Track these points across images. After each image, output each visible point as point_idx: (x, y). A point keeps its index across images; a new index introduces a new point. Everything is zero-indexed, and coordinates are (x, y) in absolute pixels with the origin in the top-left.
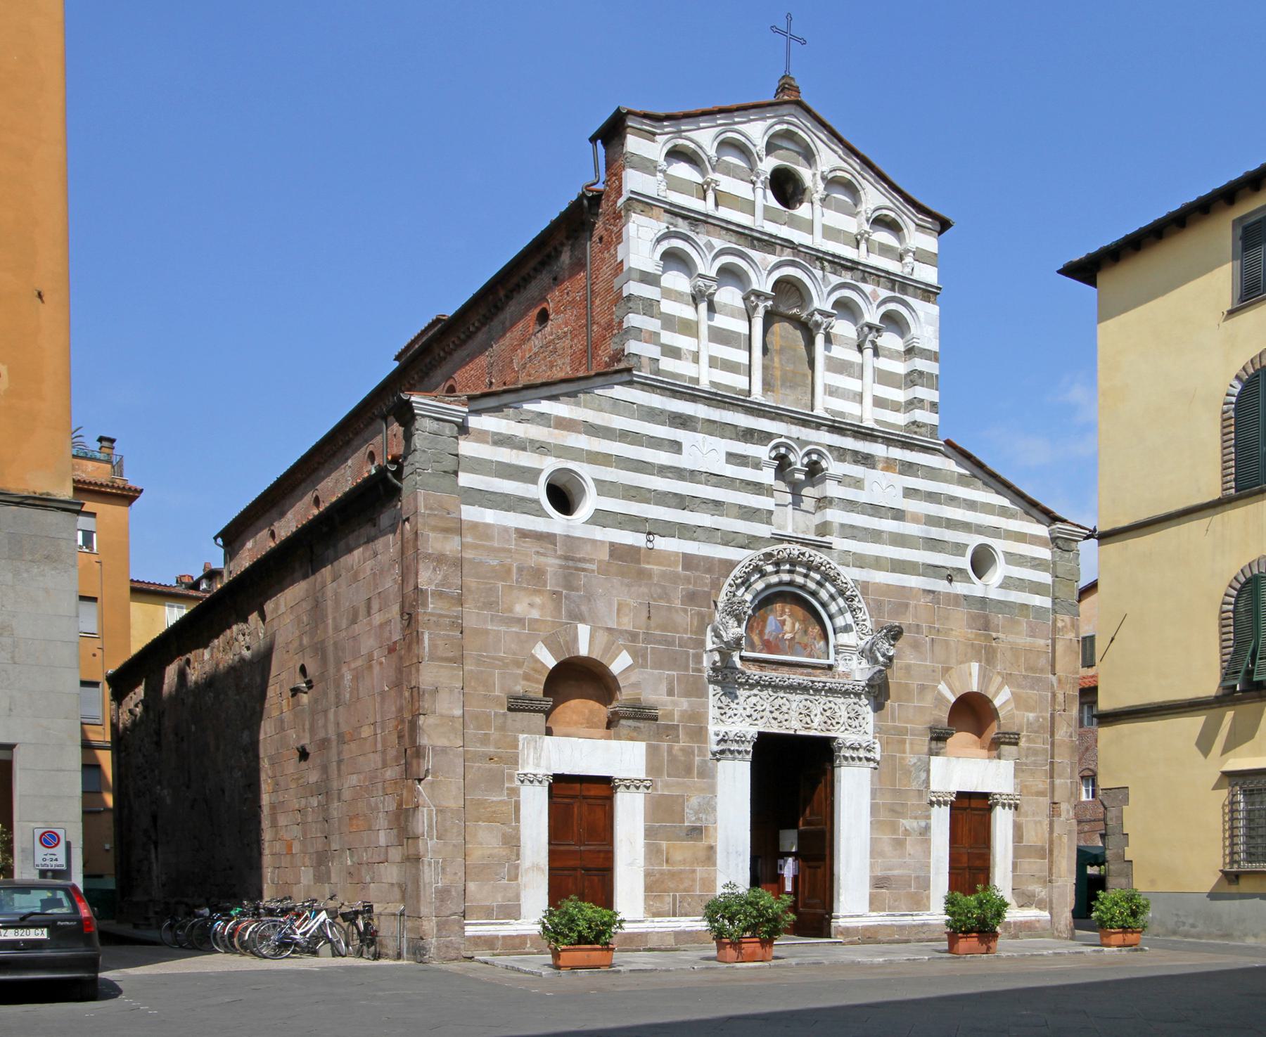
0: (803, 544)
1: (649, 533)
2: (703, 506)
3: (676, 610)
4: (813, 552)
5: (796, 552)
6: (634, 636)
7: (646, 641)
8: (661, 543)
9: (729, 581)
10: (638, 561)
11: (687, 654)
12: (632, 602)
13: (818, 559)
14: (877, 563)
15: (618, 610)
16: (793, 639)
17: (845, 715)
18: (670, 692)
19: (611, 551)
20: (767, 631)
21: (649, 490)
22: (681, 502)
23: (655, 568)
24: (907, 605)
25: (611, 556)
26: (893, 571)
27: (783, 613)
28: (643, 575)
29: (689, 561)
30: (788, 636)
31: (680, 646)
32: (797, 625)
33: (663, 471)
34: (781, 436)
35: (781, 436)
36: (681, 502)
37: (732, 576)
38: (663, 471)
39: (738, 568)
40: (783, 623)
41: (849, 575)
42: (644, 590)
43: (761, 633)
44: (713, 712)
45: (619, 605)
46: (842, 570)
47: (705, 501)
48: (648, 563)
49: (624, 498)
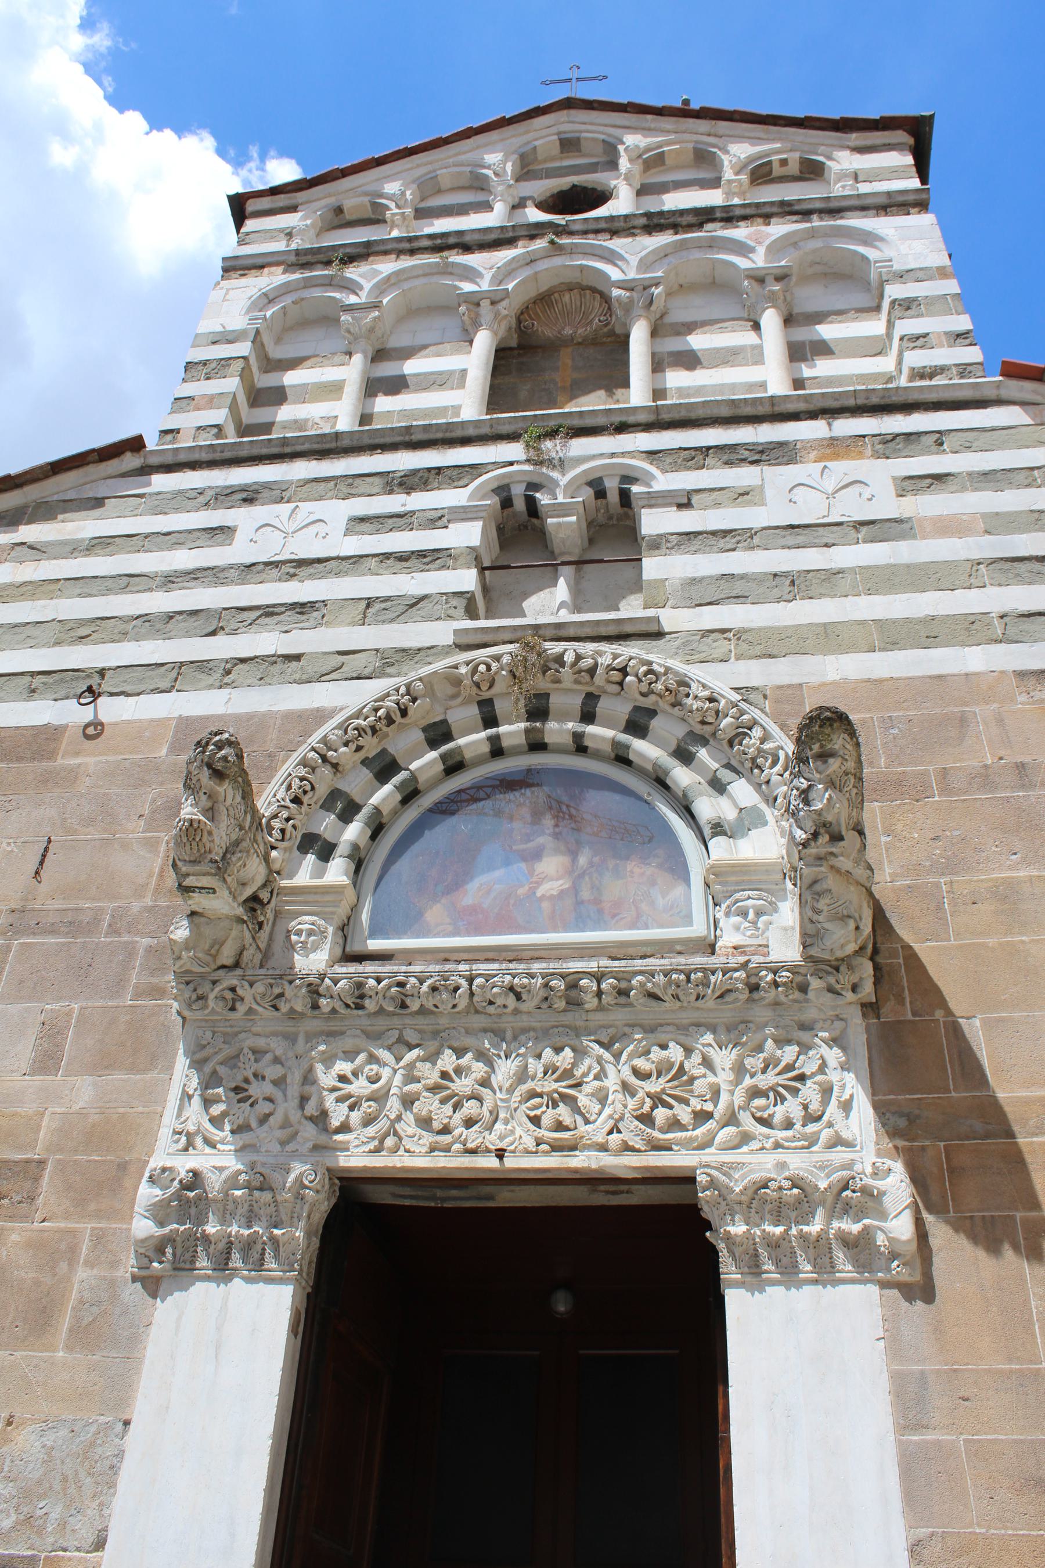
3: (125, 846)
4: (588, 648)
8: (112, 710)
10: (51, 756)
11: (130, 951)
13: (605, 660)
14: (829, 638)
17: (724, 1078)
18: (46, 1062)
24: (963, 721)
31: (113, 930)
33: (170, 580)
34: (511, 464)
35: (511, 464)
38: (170, 580)
41: (718, 678)
46: (695, 672)
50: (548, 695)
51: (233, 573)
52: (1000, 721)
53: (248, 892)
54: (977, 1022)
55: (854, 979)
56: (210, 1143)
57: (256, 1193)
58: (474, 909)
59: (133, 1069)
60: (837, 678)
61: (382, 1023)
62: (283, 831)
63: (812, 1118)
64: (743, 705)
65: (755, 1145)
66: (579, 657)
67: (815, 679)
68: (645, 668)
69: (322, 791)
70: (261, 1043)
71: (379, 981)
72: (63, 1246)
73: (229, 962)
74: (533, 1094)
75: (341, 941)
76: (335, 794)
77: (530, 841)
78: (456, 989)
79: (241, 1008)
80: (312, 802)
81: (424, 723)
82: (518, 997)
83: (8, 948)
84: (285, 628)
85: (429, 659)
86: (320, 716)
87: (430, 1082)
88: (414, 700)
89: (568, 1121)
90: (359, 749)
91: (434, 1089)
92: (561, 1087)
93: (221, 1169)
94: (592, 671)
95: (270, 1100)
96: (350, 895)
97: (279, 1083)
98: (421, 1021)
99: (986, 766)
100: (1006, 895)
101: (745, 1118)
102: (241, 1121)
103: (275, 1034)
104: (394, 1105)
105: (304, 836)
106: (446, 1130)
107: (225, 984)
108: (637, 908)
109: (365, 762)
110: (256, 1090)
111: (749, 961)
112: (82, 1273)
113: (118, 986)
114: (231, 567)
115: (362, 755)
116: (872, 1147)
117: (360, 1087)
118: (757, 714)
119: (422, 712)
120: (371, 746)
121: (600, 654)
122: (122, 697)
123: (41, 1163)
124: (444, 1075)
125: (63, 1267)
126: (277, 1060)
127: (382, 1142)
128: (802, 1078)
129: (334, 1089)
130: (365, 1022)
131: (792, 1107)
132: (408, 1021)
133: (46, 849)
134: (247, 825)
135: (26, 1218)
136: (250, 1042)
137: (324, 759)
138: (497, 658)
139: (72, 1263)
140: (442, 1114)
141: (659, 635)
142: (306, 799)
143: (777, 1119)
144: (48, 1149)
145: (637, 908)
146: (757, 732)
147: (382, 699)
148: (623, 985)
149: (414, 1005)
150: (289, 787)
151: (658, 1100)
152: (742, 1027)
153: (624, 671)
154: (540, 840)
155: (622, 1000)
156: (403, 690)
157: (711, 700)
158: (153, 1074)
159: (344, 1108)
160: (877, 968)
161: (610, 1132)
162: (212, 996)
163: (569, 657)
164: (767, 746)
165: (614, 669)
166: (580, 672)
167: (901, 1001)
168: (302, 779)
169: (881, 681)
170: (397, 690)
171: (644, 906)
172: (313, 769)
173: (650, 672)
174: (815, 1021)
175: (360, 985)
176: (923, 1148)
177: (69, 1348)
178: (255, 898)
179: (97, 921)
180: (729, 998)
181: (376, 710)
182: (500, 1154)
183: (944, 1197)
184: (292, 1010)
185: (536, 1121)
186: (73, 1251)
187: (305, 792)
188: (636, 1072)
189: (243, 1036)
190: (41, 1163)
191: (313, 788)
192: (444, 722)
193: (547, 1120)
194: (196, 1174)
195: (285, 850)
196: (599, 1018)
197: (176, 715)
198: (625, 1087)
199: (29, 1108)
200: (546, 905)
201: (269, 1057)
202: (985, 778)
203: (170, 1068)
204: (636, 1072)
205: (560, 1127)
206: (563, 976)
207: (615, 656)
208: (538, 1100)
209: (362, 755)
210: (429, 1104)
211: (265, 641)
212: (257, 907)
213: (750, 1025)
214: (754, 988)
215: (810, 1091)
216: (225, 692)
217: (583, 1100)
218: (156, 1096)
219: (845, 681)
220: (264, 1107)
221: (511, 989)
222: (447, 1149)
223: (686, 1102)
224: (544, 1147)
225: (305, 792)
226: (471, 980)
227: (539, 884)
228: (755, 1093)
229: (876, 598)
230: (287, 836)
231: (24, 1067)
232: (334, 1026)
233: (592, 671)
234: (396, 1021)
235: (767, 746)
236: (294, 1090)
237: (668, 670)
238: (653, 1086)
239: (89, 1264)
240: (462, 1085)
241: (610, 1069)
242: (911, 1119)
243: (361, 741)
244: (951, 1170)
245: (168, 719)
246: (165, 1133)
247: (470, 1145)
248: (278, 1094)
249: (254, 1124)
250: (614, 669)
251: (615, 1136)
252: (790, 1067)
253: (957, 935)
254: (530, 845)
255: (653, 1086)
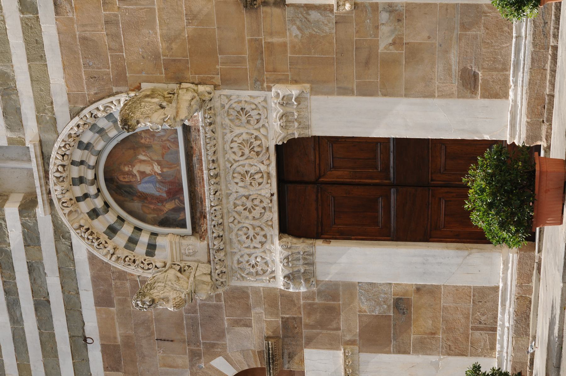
0: (47, 177)
1: (85, 339)
2: (39, 281)
5: (58, 188)
6: (195, 356)
7: (197, 343)
9: (112, 263)
10: (116, 347)
12: (160, 355)
15: (170, 367)
16: (159, 163)
19: (113, 370)
20: (157, 194)
21: (41, 334)
22: (42, 305)
23: (119, 333)
24: (84, 39)
25: (118, 370)
26: (42, 57)
27: (130, 173)
28: (128, 343)
29: (103, 300)
30: (157, 169)
31: (195, 312)
32: (141, 157)
36: (42, 305)
37: (106, 260)
39: (95, 253)
40: (143, 173)
42: (144, 342)
43: (160, 200)
44: (261, 284)
45: (165, 366)
47: (33, 281)
48: (115, 338)
49: (57, 357)
50: (72, 178)
51: (12, 297)
52: (83, 26)
53: (179, 274)
54: (219, 56)
55: (206, 94)
56: (273, 272)
57: (290, 260)
58: (168, 192)
59: (248, 297)
60: (63, 81)
61: (226, 228)
62: (148, 264)
63: (257, 108)
64: (82, 115)
65: (267, 125)
66: (58, 171)
67: (65, 89)
68: (63, 149)
69: (127, 252)
70: (235, 262)
71: (213, 232)
72: (309, 307)
73: (209, 277)
74: (251, 184)
75: (189, 237)
76: (126, 247)
77: (136, 175)
78: (215, 210)
79: (224, 270)
80: (132, 255)
81: (89, 220)
82: (216, 192)
83: (204, 343)
84: (44, 275)
85: (60, 222)
86: (92, 258)
87: (248, 213)
88: (81, 226)
89: (260, 175)
90: (106, 243)
91: (250, 212)
92: (248, 178)
93: (282, 270)
94: (63, 166)
95: (256, 258)
96: (169, 236)
97: (250, 255)
98: (225, 217)
99: (107, 35)
100: (169, 39)
101: (256, 127)
102: (264, 265)
103: (232, 259)
104: (256, 223)
105: (147, 255)
106: (264, 208)
107: (217, 278)
108: (165, 141)
109: (110, 238)
110: (253, 262)
111: (202, 126)
112: (317, 301)
113: (218, 307)
114: (7, 299)
115: (108, 241)
116: (267, 93)
117: (251, 233)
118: (86, 112)
119: (84, 220)
120: (104, 238)
121: (55, 164)
122: (85, 328)
123: (282, 318)
124: (245, 209)
125: (315, 306)
126: (242, 256)
127: (269, 226)
128: (242, 109)
129: (251, 239)
130: (226, 233)
131: (254, 113)
132: (225, 221)
133: (161, 340)
134: (163, 284)
135: (301, 318)
136: (236, 265)
137: (112, 255)
138: (59, 200)
139: (313, 304)
140: (259, 210)
141: (40, 141)
142: (133, 258)
143: (258, 117)
144: (277, 315)
145: (165, 141)
146: (95, 112)
147: (84, 238)
148: (211, 162)
149: (221, 221)
150: (130, 265)
151: (252, 149)
152: (224, 126)
153: (63, 156)
154: (135, 172)
155: (216, 161)
156: (78, 231)
157: (78, 126)
158: (250, 292)
159: (258, 237)
160: (200, 84)
161: (263, 163)
162: (221, 280)
163: (58, 175)
164: (101, 108)
165: (63, 159)
166: (64, 170)
167: (213, 78)
168: (125, 261)
169: (64, 65)
170: (78, 233)
171: (164, 139)
172: (118, 258)
173: (64, 147)
174: (221, 104)
175: (215, 238)
176: (267, 78)
177: (339, 301)
178: (180, 271)
179: (192, 318)
180: (214, 130)
181: (88, 239)
182: (272, 195)
183: (283, 75)
184: (225, 256)
185: (260, 184)
186: (310, 305)
187: (130, 259)
188: (242, 156)
189: (233, 268)
190: (282, 318)
191: (127, 256)
192: (88, 213)
193: (260, 180)
194: (285, 277)
195: (155, 262)
196: (222, 168)
197: (94, 308)
198: (246, 159)
199: (264, 325)
200: (165, 170)
201: (241, 259)
202: (114, 36)
203: (247, 287)
204: (242, 156)
205: (262, 177)
206: (209, 180)
207: (56, 158)
208: (253, 184)
209: (108, 241)
210: (256, 213)
211: (53, 283)
212: (182, 270)
213: (223, 123)
214: (210, 124)
215: (248, 107)
216: (80, 292)
217: (252, 171)
218: (256, 291)
219: (64, 78)
220: (259, 259)
221: (214, 194)
222: (270, 208)
223: (251, 143)
224: (269, 181)
225: (130, 259)
226: (212, 206)
227: (155, 172)
228: (248, 122)
229: (14, 59)
230: (149, 262)
231: (250, 329)
232: (228, 241)
233: (63, 166)
234: (226, 224)
235: (101, 108)
236: (253, 251)
237: (63, 141)
238: (247, 151)
239: (314, 299)
240: (249, 204)
241: (241, 163)
242: (256, 81)
243: (103, 242)
244: (275, 72)
245: (96, 310)
246: (271, 285)
247: (269, 202)
248: (254, 255)
249: (265, 261)
250: (63, 159)
251: (264, 162)
252: (238, 112)
253: (187, 57)
254: (137, 175)
255: (247, 151)
